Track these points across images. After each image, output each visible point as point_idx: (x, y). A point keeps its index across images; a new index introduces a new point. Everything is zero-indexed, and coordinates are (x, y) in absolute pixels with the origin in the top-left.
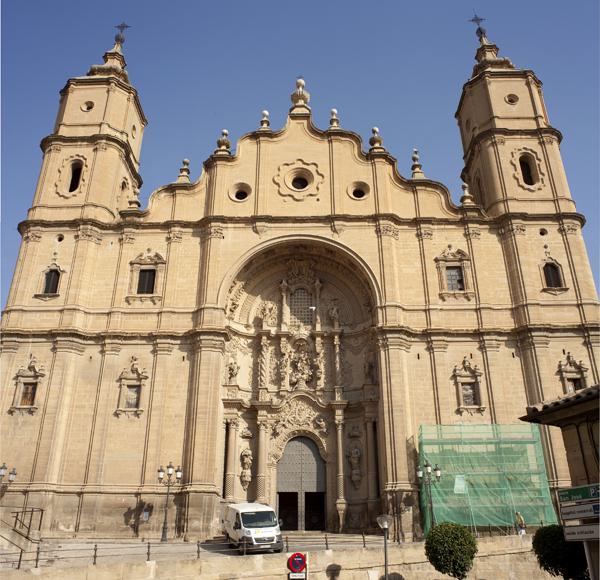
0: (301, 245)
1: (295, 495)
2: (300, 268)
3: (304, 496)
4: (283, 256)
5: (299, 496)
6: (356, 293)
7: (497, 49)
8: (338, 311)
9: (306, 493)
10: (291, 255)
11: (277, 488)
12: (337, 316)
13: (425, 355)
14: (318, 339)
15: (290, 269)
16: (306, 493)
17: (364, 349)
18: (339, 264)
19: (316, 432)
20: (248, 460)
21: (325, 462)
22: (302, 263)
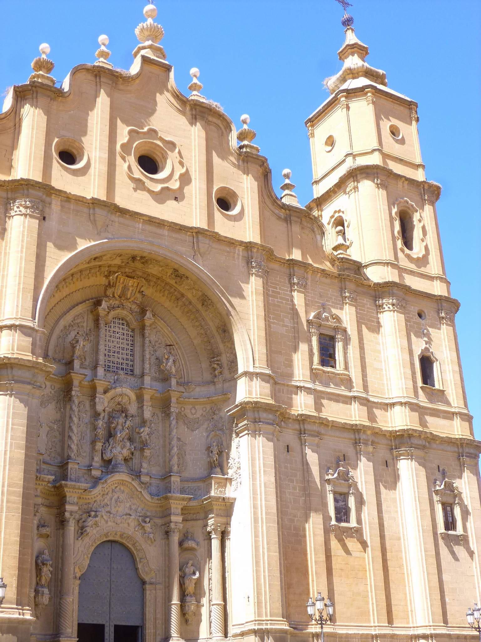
0: (142, 257)
1: (101, 628)
2: (125, 288)
3: (112, 629)
4: (109, 266)
5: (107, 629)
7: (367, 53)
8: (174, 361)
9: (117, 627)
10: (120, 267)
11: (79, 616)
12: (174, 370)
13: (294, 443)
14: (147, 397)
15: (109, 285)
16: (117, 627)
17: (205, 426)
18: (183, 295)
19: (138, 536)
20: (46, 571)
21: (144, 583)
22: (131, 282)
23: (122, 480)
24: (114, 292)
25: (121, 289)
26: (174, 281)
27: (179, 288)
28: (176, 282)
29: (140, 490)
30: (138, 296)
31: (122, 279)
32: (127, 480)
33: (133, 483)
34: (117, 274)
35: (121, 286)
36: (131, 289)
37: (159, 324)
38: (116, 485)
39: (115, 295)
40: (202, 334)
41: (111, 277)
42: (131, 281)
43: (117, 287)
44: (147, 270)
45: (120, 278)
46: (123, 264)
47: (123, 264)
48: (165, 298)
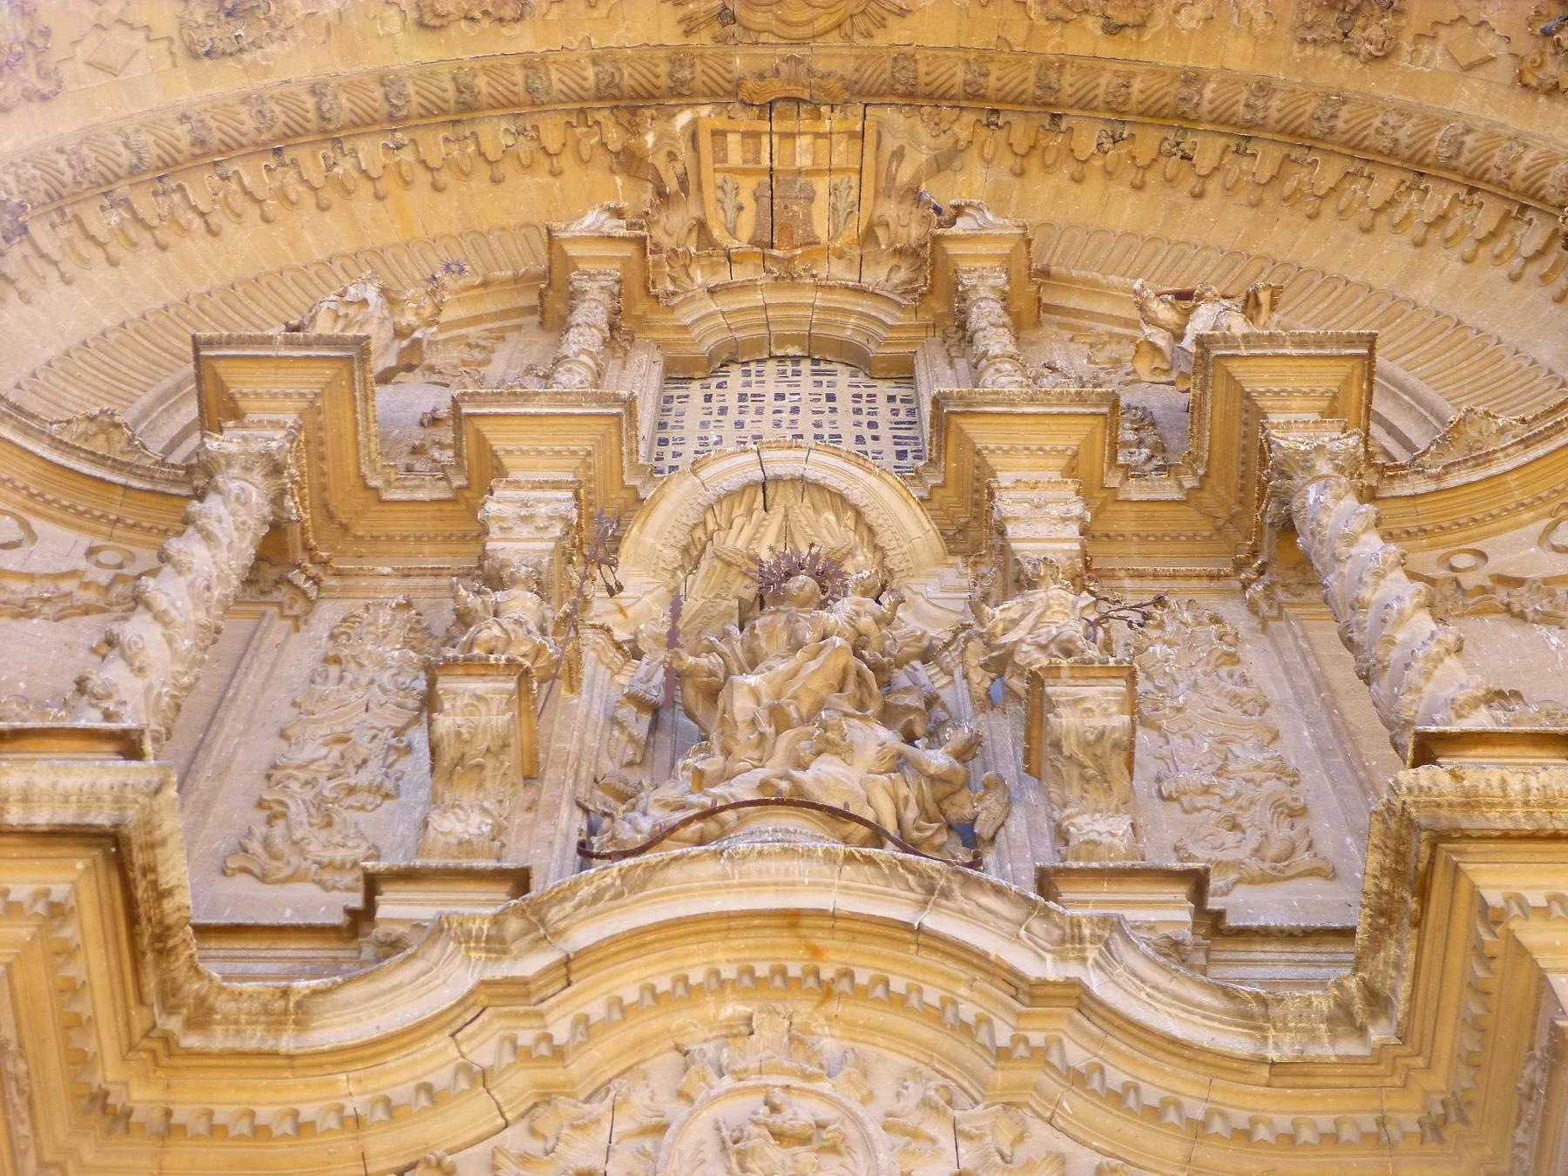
6: (1426, 291)
23: (792, 919)
24: (702, 226)
25: (746, 198)
26: (1093, 24)
27: (1146, 56)
28: (1113, 29)
29: (1051, 970)
30: (890, 210)
31: (733, 139)
32: (848, 904)
33: (932, 921)
34: (683, 118)
35: (748, 185)
36: (821, 185)
37: (1104, 307)
38: (733, 1009)
39: (717, 233)
40: (1442, 218)
41: (650, 139)
42: (803, 142)
43: (710, 193)
44: (881, 40)
45: (720, 134)
46: (703, 39)
47: (703, 39)
48: (1095, 183)
